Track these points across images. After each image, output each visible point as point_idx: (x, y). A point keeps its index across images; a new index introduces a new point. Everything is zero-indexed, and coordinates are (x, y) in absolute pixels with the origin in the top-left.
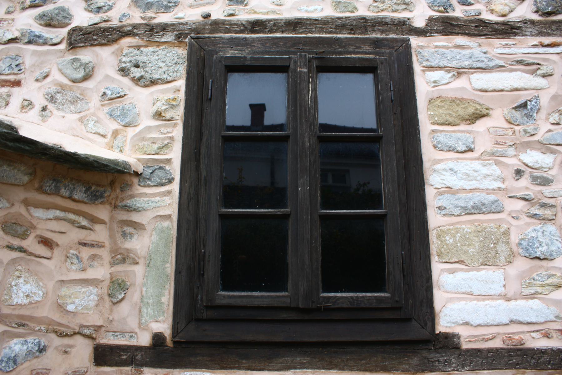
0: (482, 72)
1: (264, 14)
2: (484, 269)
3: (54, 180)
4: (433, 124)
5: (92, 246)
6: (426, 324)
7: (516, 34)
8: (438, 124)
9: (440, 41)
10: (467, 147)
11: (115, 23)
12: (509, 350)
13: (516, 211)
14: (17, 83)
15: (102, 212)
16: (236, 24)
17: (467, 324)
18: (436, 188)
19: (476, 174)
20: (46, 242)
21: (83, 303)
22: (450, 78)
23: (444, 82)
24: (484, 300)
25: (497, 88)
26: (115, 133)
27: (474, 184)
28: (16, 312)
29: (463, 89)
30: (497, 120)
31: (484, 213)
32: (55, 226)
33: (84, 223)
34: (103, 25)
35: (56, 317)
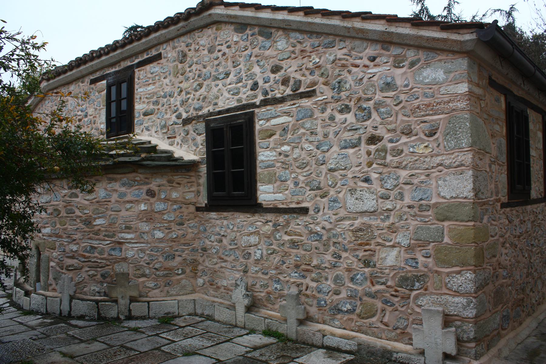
7: (285, 101)
11: (190, 117)
14: (175, 137)
15: (192, 174)
20: (179, 184)
21: (190, 196)
26: (195, 150)
27: (268, 159)
33: (188, 177)
35: (183, 200)
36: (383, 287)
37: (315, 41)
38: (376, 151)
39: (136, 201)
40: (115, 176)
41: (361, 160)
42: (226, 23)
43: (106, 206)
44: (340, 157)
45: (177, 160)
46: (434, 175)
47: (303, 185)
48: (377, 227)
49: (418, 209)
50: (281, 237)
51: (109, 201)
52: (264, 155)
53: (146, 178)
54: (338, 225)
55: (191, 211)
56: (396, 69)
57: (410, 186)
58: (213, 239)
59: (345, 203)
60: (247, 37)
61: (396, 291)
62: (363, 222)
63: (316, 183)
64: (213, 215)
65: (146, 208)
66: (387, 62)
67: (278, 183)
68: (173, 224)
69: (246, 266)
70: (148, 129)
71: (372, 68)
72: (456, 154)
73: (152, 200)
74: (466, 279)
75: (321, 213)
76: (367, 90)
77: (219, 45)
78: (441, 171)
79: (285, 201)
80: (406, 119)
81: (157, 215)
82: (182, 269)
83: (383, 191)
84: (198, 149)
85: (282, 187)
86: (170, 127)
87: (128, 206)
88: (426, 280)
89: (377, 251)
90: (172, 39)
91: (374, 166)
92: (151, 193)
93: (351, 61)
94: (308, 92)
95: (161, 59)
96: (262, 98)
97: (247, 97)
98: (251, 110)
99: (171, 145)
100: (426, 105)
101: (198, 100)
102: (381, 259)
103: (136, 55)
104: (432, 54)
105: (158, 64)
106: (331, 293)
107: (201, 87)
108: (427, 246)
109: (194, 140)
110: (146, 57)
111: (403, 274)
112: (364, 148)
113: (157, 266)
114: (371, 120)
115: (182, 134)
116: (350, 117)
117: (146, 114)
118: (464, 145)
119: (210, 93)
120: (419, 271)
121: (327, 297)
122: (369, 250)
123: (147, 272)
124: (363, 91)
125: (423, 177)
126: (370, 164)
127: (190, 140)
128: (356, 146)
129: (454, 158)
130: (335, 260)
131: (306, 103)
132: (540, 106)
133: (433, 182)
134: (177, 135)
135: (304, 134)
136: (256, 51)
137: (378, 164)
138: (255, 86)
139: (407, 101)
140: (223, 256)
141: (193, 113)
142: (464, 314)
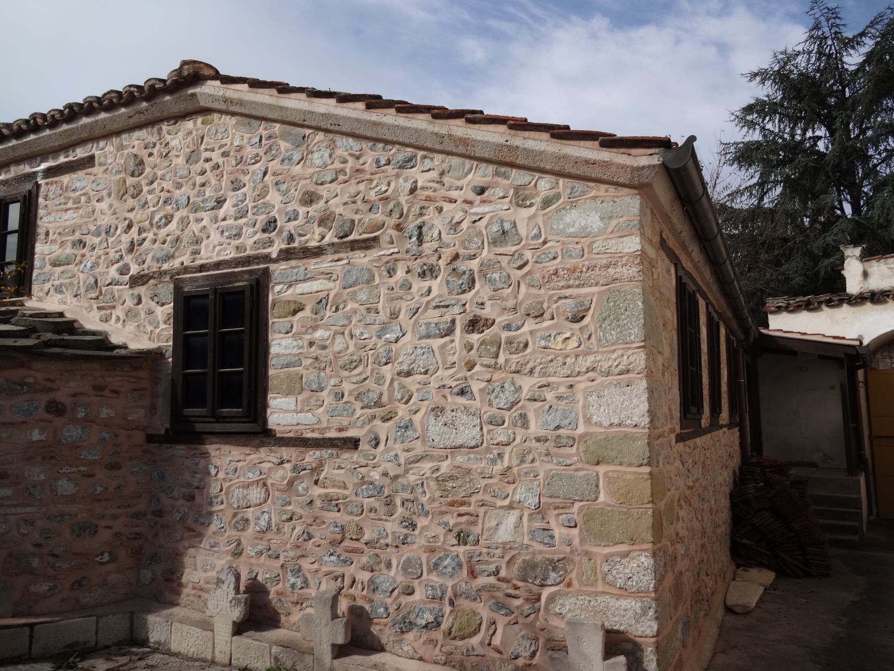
5: (140, 390)
7: (323, 254)
9: (283, 266)
11: (146, 272)
12: (296, 438)
14: (114, 307)
15: (143, 374)
20: (115, 392)
27: (288, 351)
30: (307, 313)
33: (134, 380)
34: (142, 273)
36: (492, 580)
37: (381, 153)
38: (481, 344)
39: (23, 423)
41: (455, 358)
42: (221, 112)
44: (419, 351)
46: (582, 386)
47: (352, 399)
48: (481, 473)
49: (553, 444)
50: (307, 489)
52: (280, 345)
54: (412, 468)
56: (519, 208)
57: (538, 404)
58: (175, 494)
59: (425, 430)
60: (260, 141)
61: (516, 588)
62: (456, 463)
63: (373, 396)
64: (180, 450)
65: (43, 438)
66: (504, 197)
67: (305, 394)
69: (239, 544)
71: (478, 206)
72: (620, 352)
73: (58, 422)
74: (638, 566)
75: (381, 447)
76: (470, 241)
77: (206, 150)
78: (593, 381)
79: (317, 426)
80: (534, 291)
82: (111, 554)
83: (494, 411)
84: (158, 331)
85: (313, 402)
86: (104, 289)
88: (569, 568)
89: (481, 515)
90: (118, 133)
91: (477, 368)
93: (443, 192)
94: (365, 241)
95: (94, 166)
96: (284, 246)
97: (255, 243)
98: (262, 266)
100: (568, 270)
101: (164, 243)
102: (489, 529)
103: (44, 155)
104: (580, 186)
105: (87, 174)
106: (396, 592)
108: (569, 507)
109: (150, 312)
110: (62, 159)
111: (528, 558)
112: (461, 337)
113: (59, 550)
114: (473, 292)
116: (436, 285)
117: (55, 264)
118: (632, 337)
120: (555, 553)
121: (389, 601)
122: (467, 514)
123: (35, 563)
124: (463, 243)
125: (562, 389)
126: (470, 366)
128: (446, 335)
129: (615, 360)
130: (405, 531)
131: (361, 258)
132: (704, 288)
133: (580, 397)
135: (355, 312)
136: (274, 165)
137: (486, 366)
138: (270, 225)
139: (537, 262)
140: (194, 526)
141: (150, 265)
142: (637, 630)
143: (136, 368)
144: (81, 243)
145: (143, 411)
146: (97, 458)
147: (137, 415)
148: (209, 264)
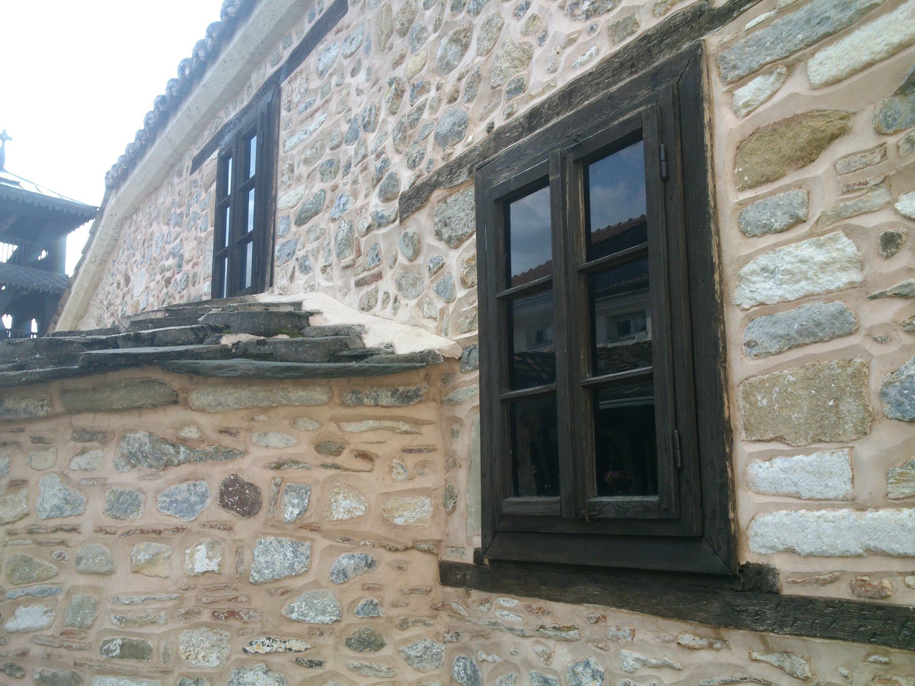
0: (831, 43)
1: (539, 95)
2: (817, 450)
3: (353, 392)
4: (742, 189)
5: (420, 451)
6: (719, 548)
8: (751, 187)
10: (792, 216)
11: (426, 176)
12: (862, 607)
13: (882, 326)
14: (378, 276)
15: (425, 411)
16: (515, 127)
17: (791, 551)
18: (744, 310)
19: (804, 267)
20: (364, 456)
22: (773, 83)
23: (763, 97)
24: (819, 508)
25: (857, 65)
26: (442, 312)
27: (805, 286)
28: (338, 527)
29: (793, 96)
31: (821, 341)
32: (371, 437)
33: (406, 427)
34: (419, 182)
35: (381, 531)
39: (178, 530)
40: (102, 422)
43: (59, 550)
45: (365, 354)
51: (73, 529)
53: (225, 431)
55: (414, 582)
64: (507, 608)
65: (213, 566)
68: (330, 641)
70: (305, 269)
73: (245, 528)
81: (260, 600)
87: (143, 551)
92: (240, 498)
98: (685, 46)
99: (366, 307)
101: (453, 100)
105: (338, 31)
107: (466, 47)
109: (438, 268)
115: (402, 260)
119: (498, 51)
127: (426, 274)
134: (384, 266)
141: (435, 158)
143: (407, 398)
144: (331, 168)
145: (428, 501)
146: (327, 619)
147: (415, 514)
148: (549, 102)
